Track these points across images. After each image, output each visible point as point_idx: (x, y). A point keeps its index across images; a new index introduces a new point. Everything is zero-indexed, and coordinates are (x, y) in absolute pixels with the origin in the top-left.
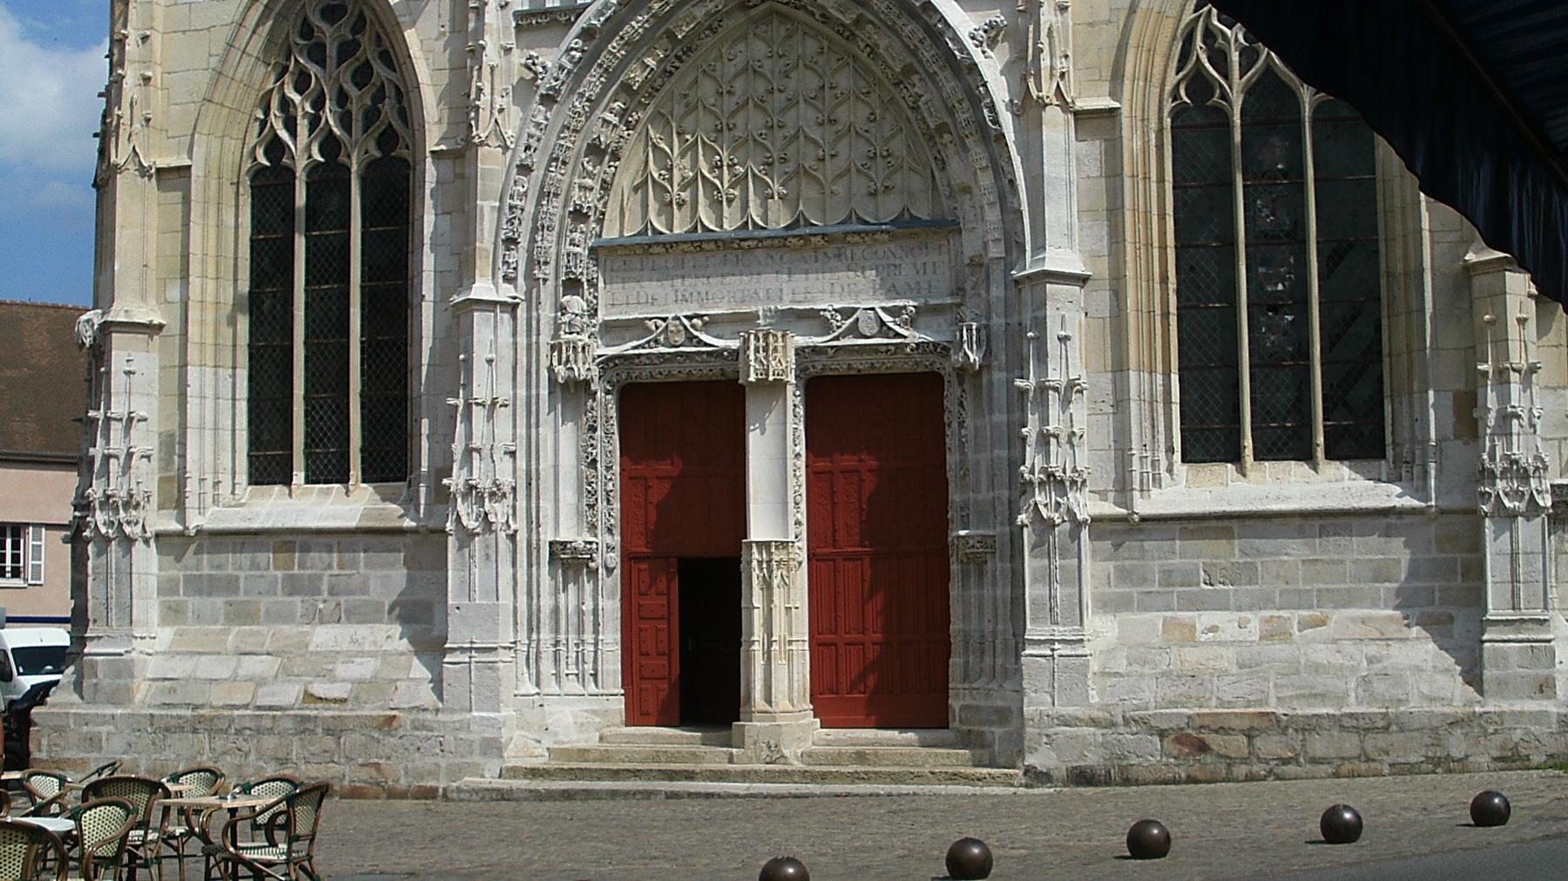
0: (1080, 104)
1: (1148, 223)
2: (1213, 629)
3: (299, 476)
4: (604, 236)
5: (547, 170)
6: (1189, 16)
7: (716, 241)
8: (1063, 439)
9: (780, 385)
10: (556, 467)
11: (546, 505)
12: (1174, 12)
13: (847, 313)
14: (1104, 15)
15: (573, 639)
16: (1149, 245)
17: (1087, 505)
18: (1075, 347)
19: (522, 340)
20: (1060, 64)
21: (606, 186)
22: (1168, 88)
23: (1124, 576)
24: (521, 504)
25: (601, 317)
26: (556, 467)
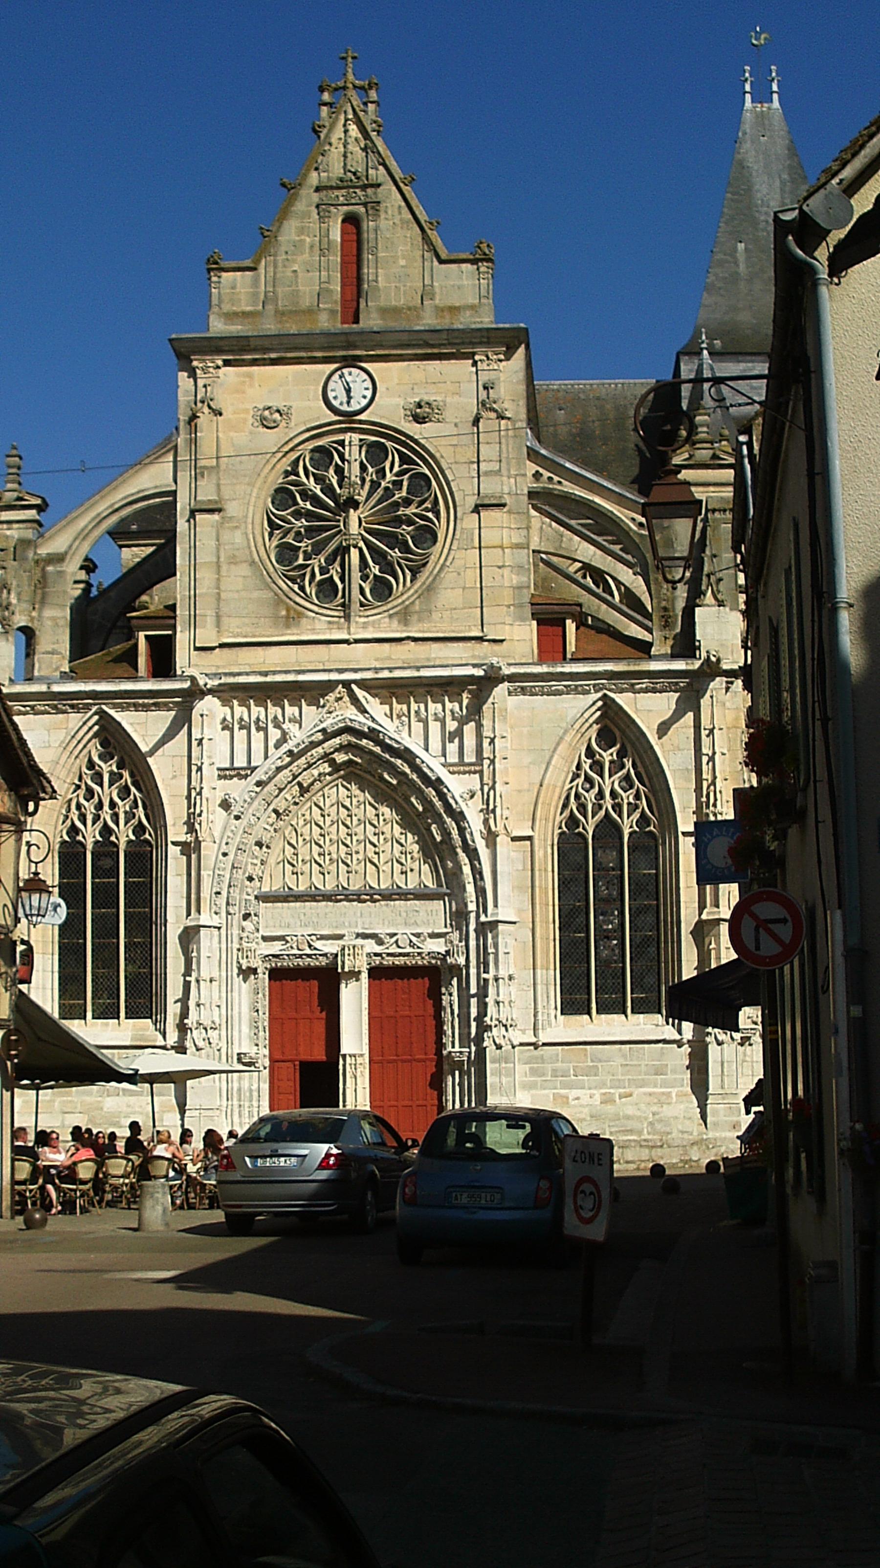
0: (516, 833)
1: (547, 893)
2: (578, 1099)
3: (89, 1015)
4: (263, 890)
5: (236, 855)
6: (568, 786)
7: (323, 896)
8: (507, 1004)
9: (359, 972)
10: (240, 1013)
11: (236, 1033)
12: (560, 784)
13: (392, 935)
14: (526, 786)
15: (247, 1104)
16: (548, 905)
17: (517, 1036)
18: (512, 955)
19: (224, 946)
20: (506, 813)
21: (263, 863)
22: (556, 823)
23: (533, 1072)
24: (224, 1033)
25: (261, 932)
26: (240, 1013)
